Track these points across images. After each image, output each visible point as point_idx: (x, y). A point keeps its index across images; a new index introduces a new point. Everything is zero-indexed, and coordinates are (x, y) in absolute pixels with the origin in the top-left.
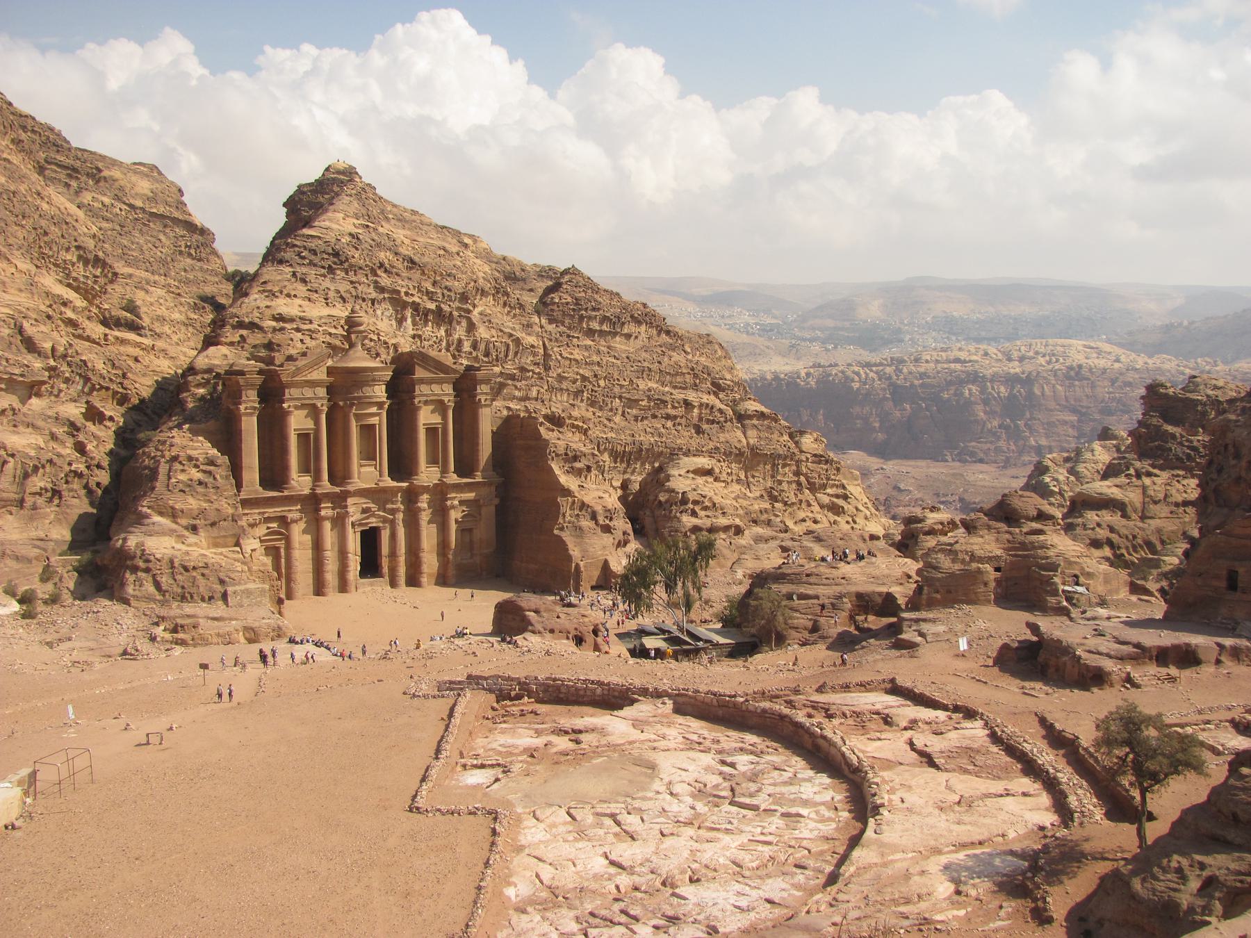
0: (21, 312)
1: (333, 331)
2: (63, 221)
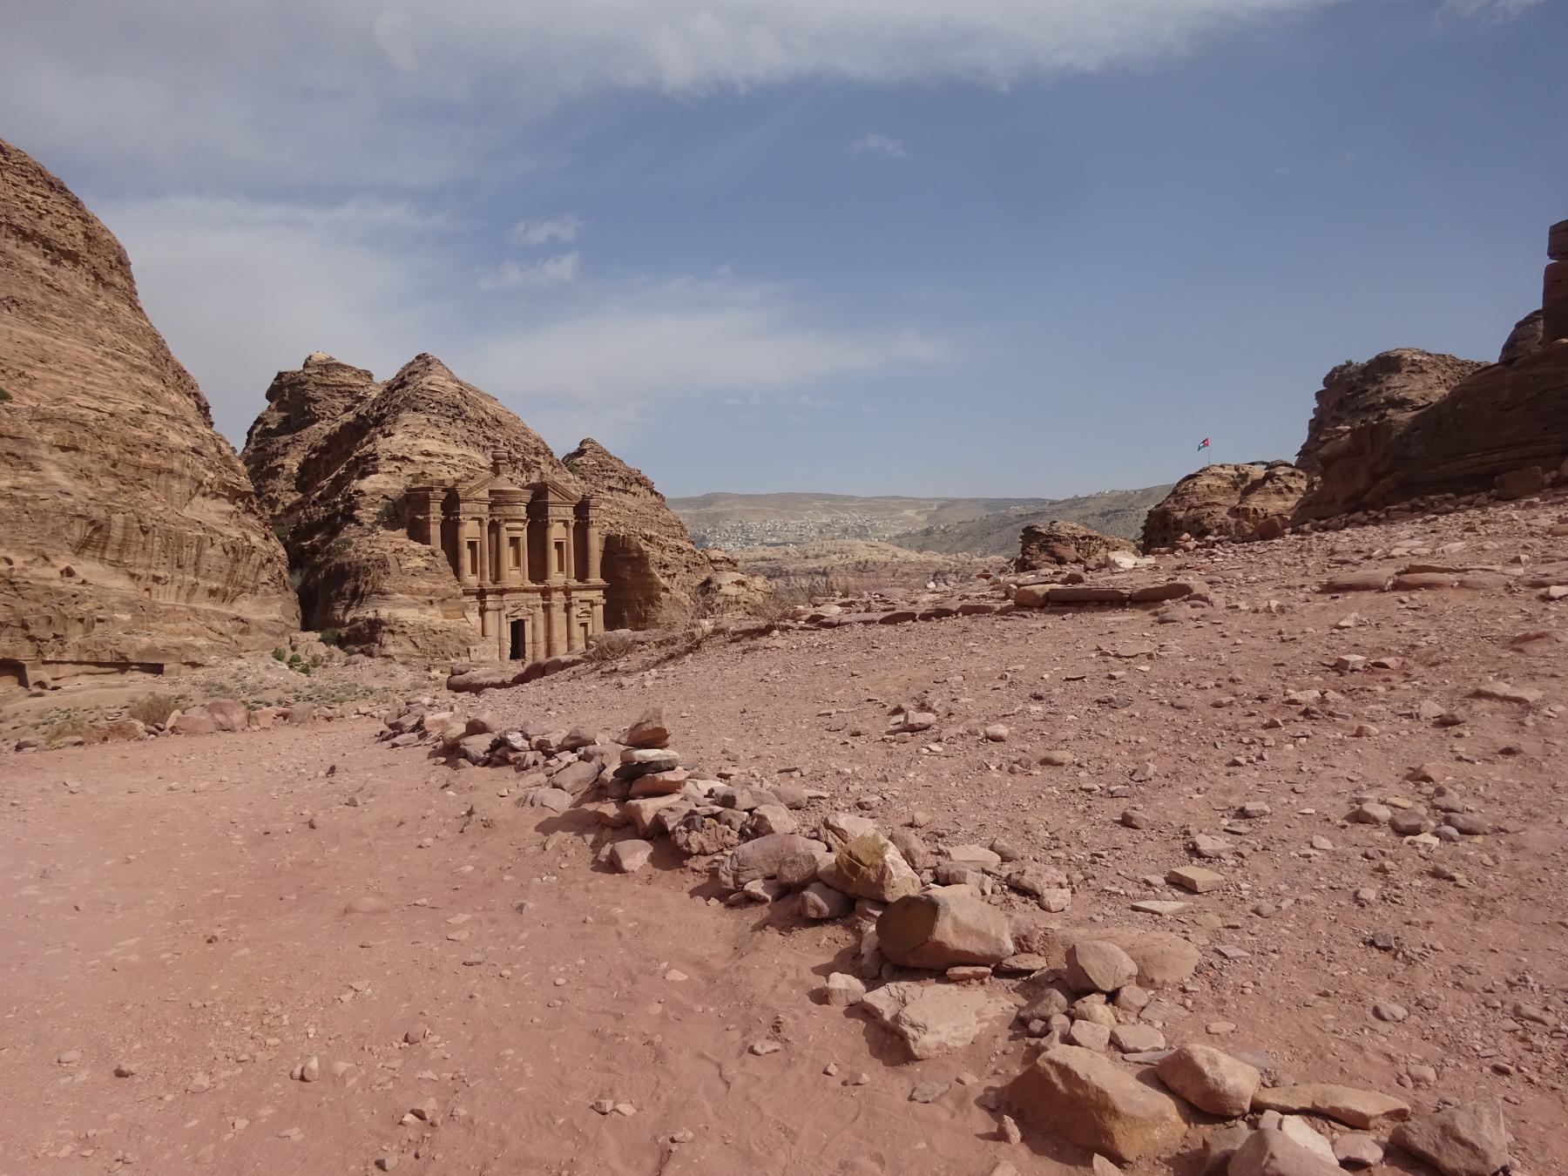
1: (470, 467)
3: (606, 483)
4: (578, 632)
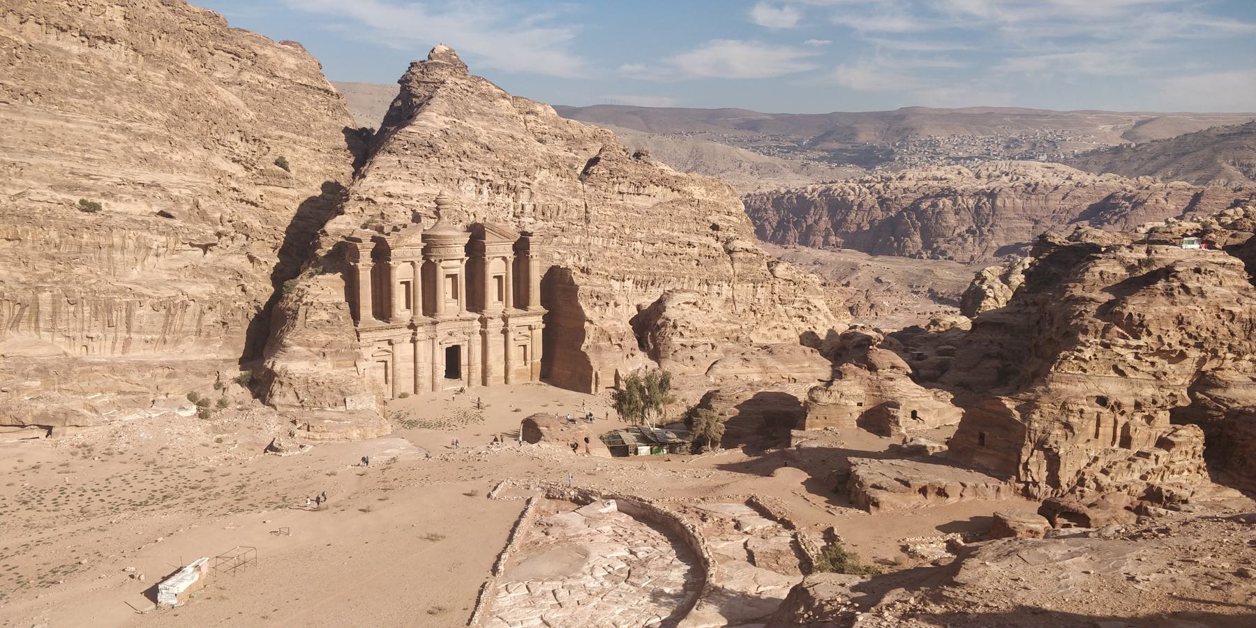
0: (197, 192)
1: (428, 205)
2: (225, 112)
3: (616, 189)
4: (515, 353)
